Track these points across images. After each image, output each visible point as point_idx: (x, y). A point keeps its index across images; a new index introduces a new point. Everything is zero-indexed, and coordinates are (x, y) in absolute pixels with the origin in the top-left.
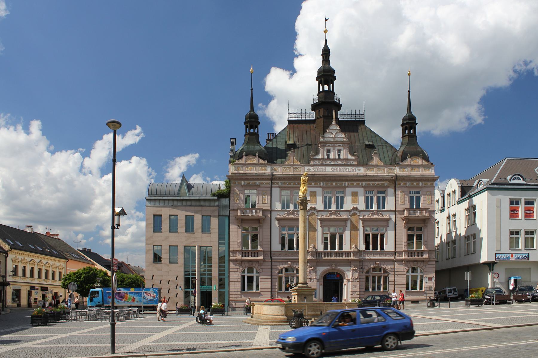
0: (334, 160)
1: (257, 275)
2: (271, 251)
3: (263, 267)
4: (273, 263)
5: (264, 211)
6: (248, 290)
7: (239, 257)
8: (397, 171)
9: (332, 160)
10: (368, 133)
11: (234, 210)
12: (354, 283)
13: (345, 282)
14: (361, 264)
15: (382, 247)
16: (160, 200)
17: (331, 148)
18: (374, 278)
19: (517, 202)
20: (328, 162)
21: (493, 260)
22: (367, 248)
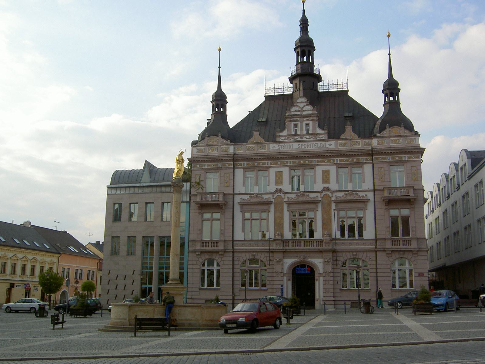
0: (302, 135)
1: (218, 268)
2: (233, 241)
3: (223, 259)
4: (235, 254)
5: (224, 195)
7: (199, 247)
8: (375, 142)
9: (299, 135)
11: (194, 195)
14: (335, 254)
15: (361, 235)
17: (299, 123)
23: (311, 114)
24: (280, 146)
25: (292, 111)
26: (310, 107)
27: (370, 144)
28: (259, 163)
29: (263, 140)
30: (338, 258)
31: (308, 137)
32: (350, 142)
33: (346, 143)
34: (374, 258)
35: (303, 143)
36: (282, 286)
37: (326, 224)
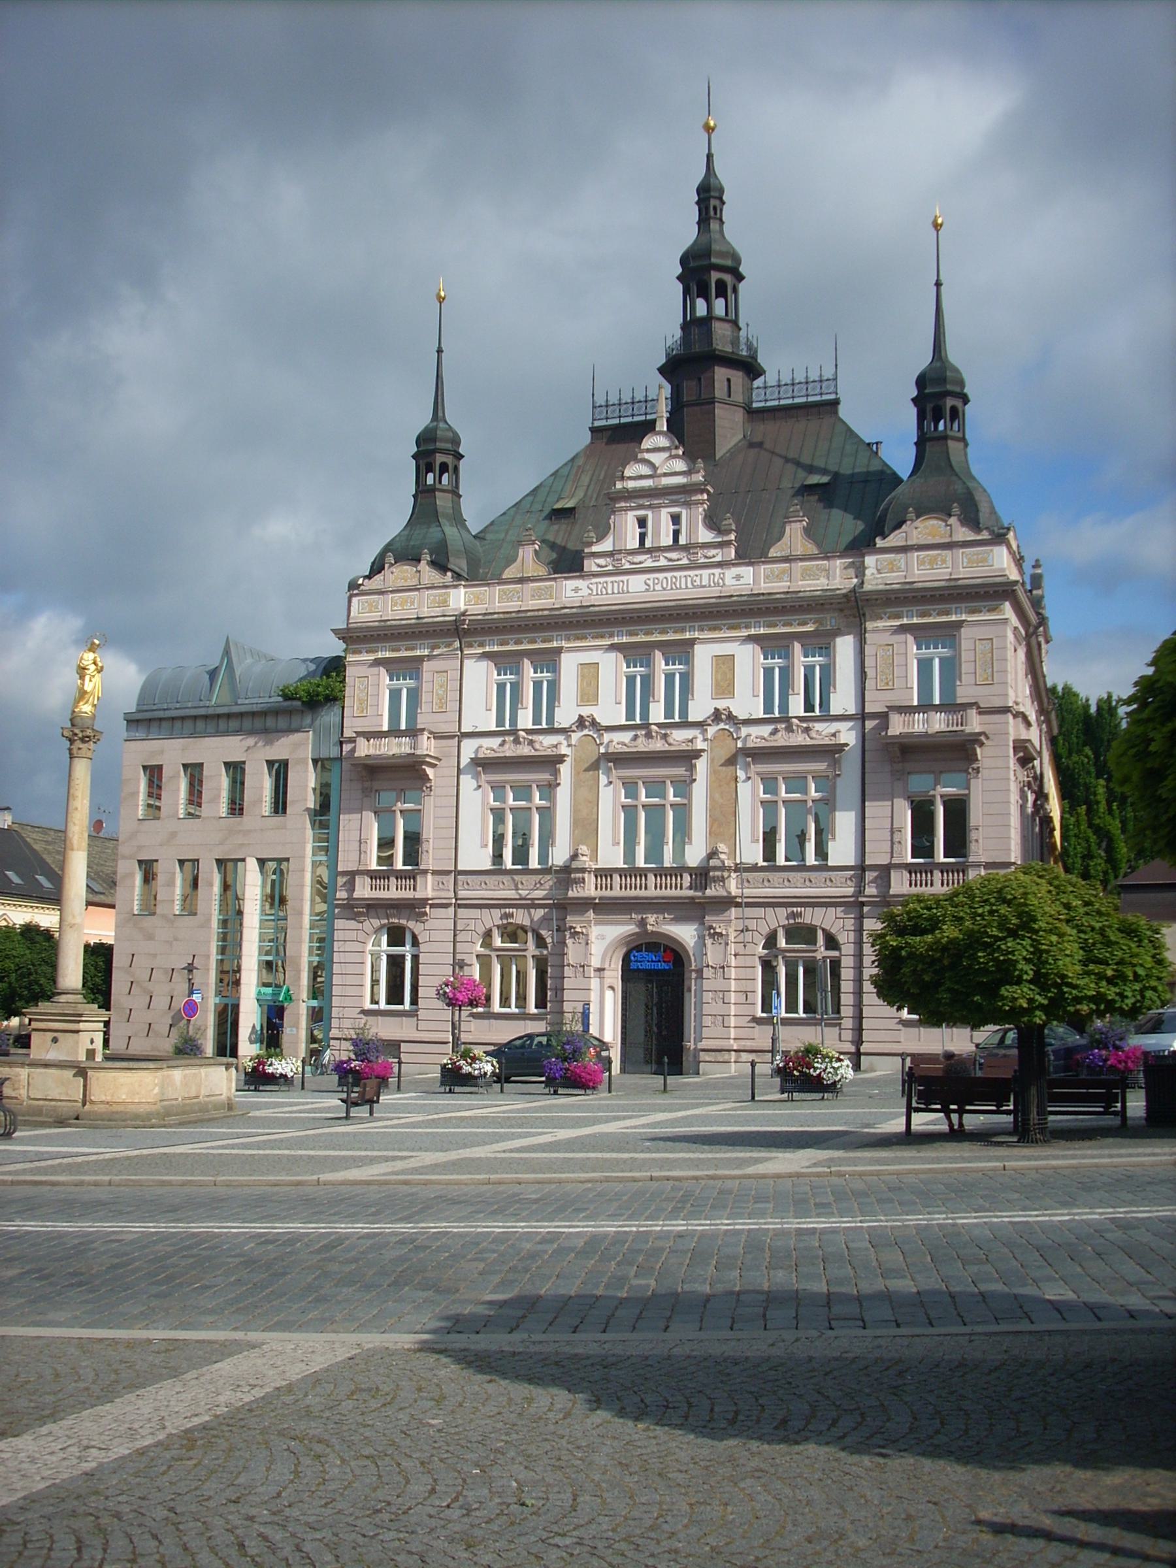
6: (388, 1002)
7: (364, 890)
16: (161, 719)
17: (649, 513)
23: (684, 486)
24: (594, 587)
25: (630, 478)
26: (680, 465)
28: (524, 640)
29: (542, 571)
30: (752, 924)
33: (783, 572)
35: (661, 576)
36: (587, 1004)
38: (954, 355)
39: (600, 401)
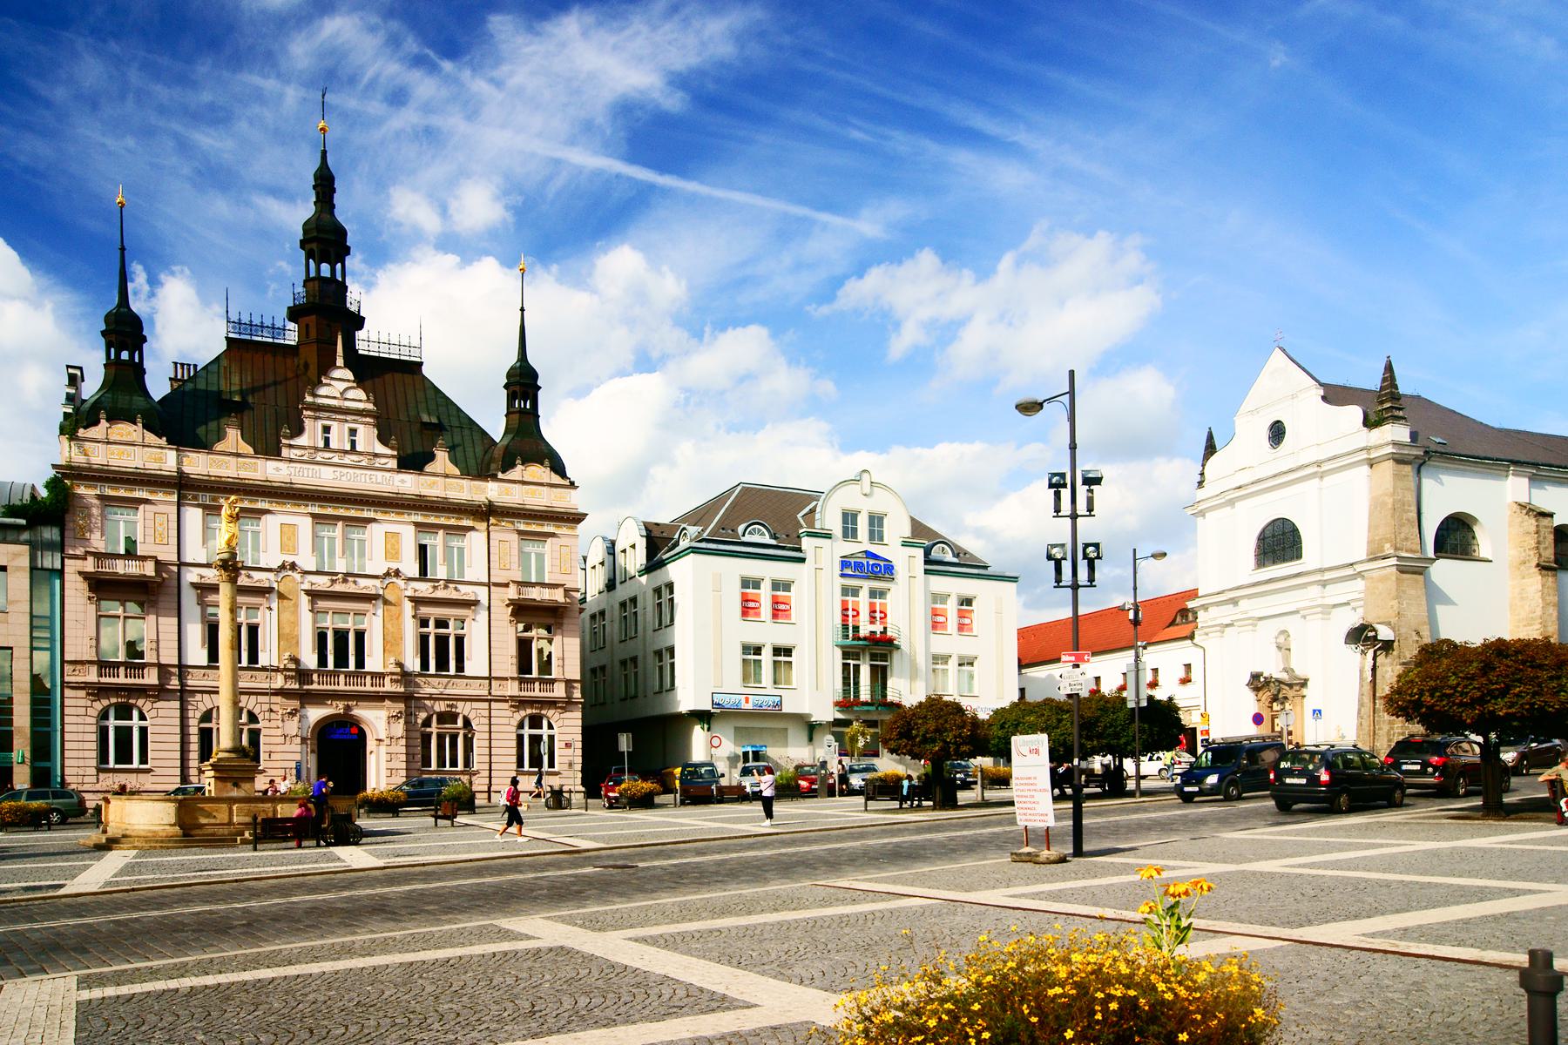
5: (160, 565)
10: (430, 393)
12: (393, 749)
13: (371, 744)
17: (335, 426)
18: (441, 737)
19: (756, 584)
20: (327, 455)
21: (707, 706)
22: (425, 665)
26: (361, 394)
27: (484, 491)
31: (355, 457)
32: (443, 479)
34: (486, 713)
37: (391, 642)
38: (532, 359)
39: (234, 318)
